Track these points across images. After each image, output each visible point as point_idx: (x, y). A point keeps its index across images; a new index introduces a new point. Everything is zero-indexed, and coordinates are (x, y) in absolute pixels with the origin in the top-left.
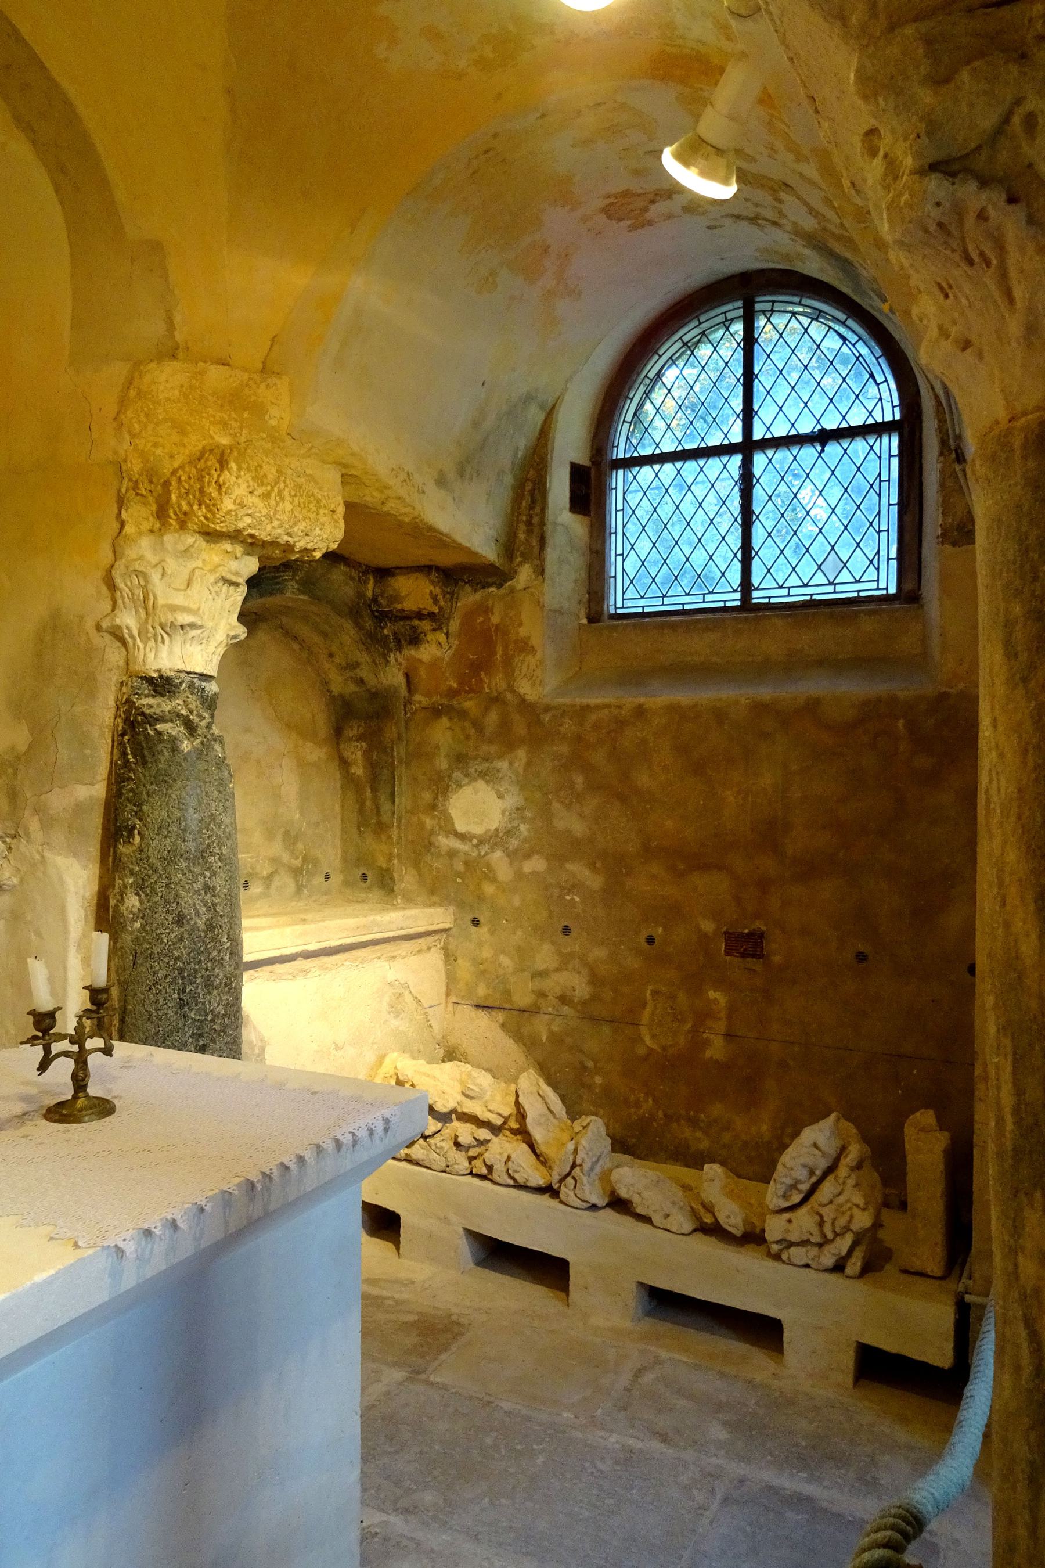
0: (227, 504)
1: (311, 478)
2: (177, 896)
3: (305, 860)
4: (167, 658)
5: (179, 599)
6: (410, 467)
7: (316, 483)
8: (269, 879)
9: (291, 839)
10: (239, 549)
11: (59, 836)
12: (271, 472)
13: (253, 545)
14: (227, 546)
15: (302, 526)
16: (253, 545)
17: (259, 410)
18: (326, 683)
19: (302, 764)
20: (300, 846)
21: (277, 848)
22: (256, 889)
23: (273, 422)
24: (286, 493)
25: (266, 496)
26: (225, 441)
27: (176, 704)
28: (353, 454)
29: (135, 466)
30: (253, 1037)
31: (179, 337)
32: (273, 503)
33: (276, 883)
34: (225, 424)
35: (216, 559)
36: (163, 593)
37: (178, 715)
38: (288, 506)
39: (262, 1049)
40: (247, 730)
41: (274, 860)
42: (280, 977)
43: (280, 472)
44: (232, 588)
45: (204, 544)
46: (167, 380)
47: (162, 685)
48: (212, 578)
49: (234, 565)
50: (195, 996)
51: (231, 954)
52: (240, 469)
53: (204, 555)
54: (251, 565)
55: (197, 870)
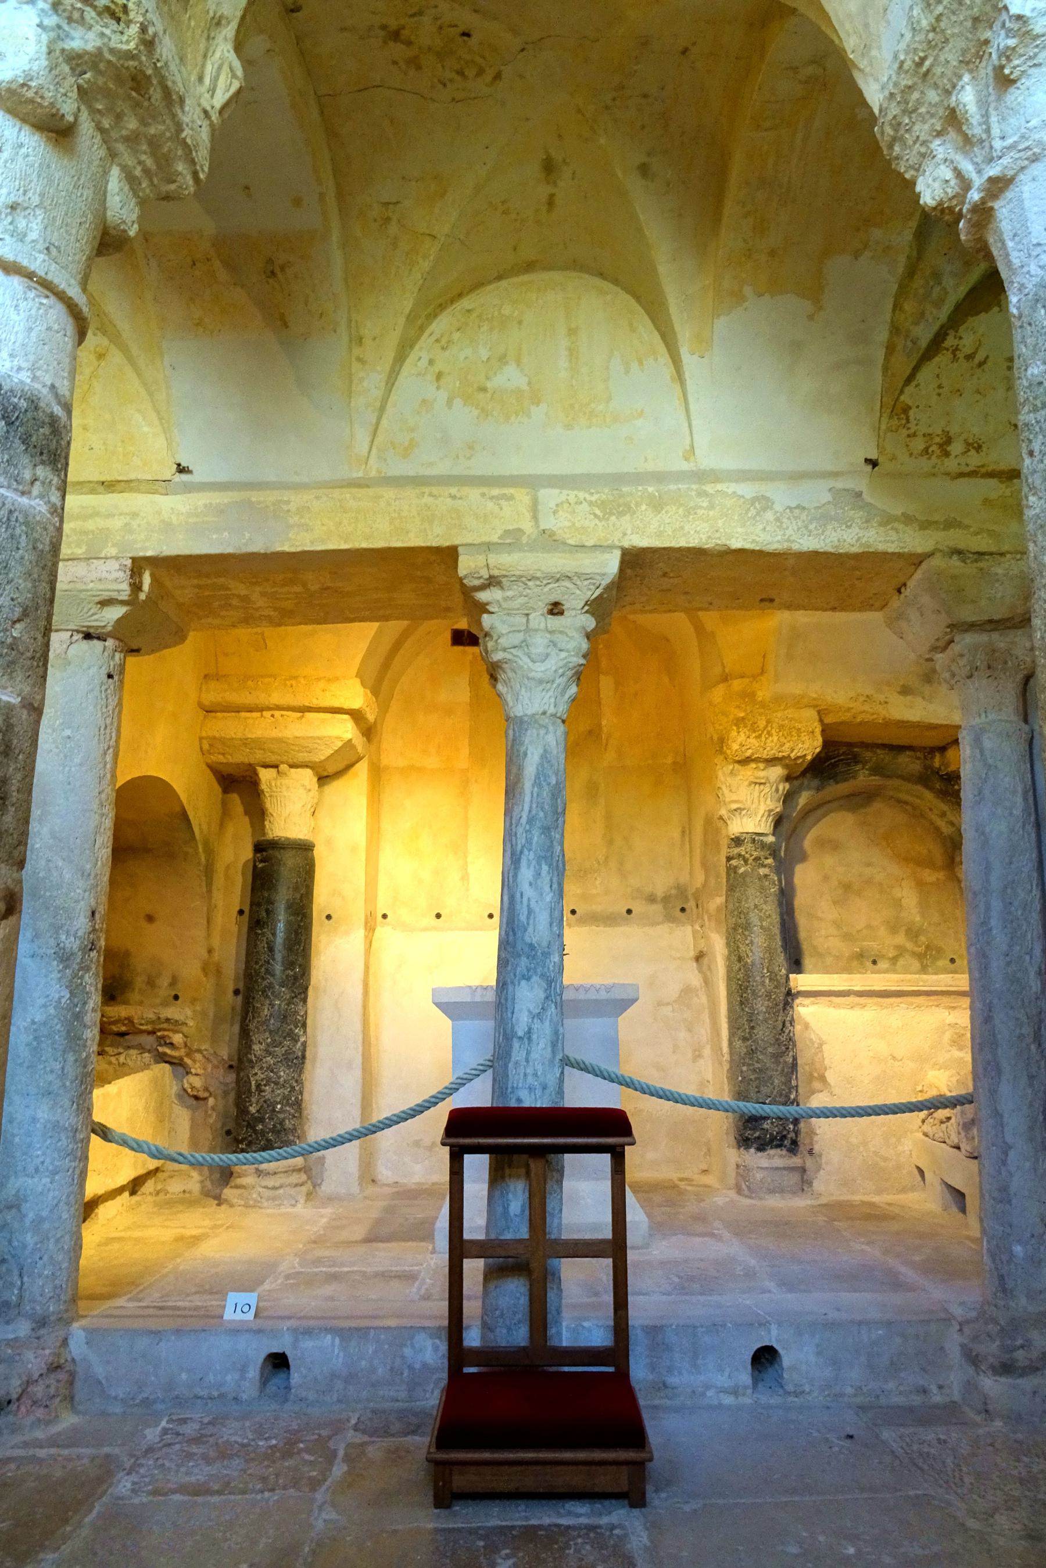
0: (735, 747)
1: (791, 720)
2: (738, 947)
3: (928, 947)
4: (738, 826)
5: (734, 797)
6: (869, 691)
7: (796, 721)
8: (894, 960)
9: (913, 933)
10: (762, 766)
11: (713, 924)
12: (762, 723)
13: (771, 761)
14: (753, 765)
15: (787, 745)
16: (771, 761)
17: (752, 695)
18: (937, 829)
19: (920, 885)
20: (923, 938)
21: (901, 939)
22: (883, 965)
23: (760, 699)
24: (773, 731)
25: (759, 737)
26: (742, 715)
27: (742, 850)
28: (814, 699)
29: (715, 737)
30: (813, 1036)
31: (727, 670)
32: (763, 739)
33: (901, 962)
34: (738, 707)
35: (749, 773)
36: (729, 796)
37: (740, 855)
38: (775, 738)
39: (821, 1045)
40: (869, 865)
41: (897, 947)
42: (837, 1006)
43: (768, 722)
44: (762, 787)
45: (740, 767)
46: (718, 693)
47: (737, 841)
48: (746, 783)
49: (762, 774)
50: (747, 1000)
51: (770, 979)
52: (738, 728)
53: (742, 773)
54: (777, 772)
55: (747, 933)
